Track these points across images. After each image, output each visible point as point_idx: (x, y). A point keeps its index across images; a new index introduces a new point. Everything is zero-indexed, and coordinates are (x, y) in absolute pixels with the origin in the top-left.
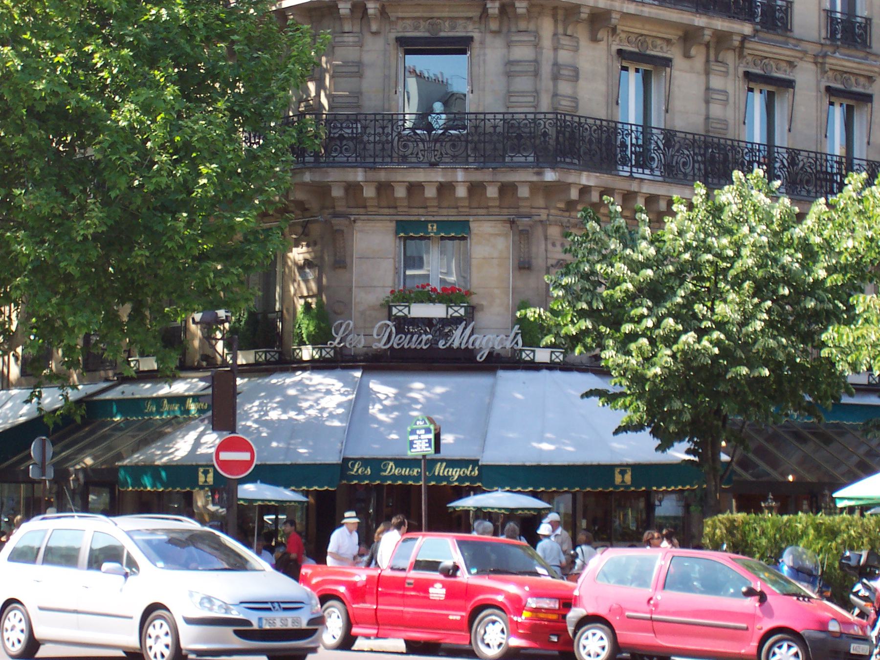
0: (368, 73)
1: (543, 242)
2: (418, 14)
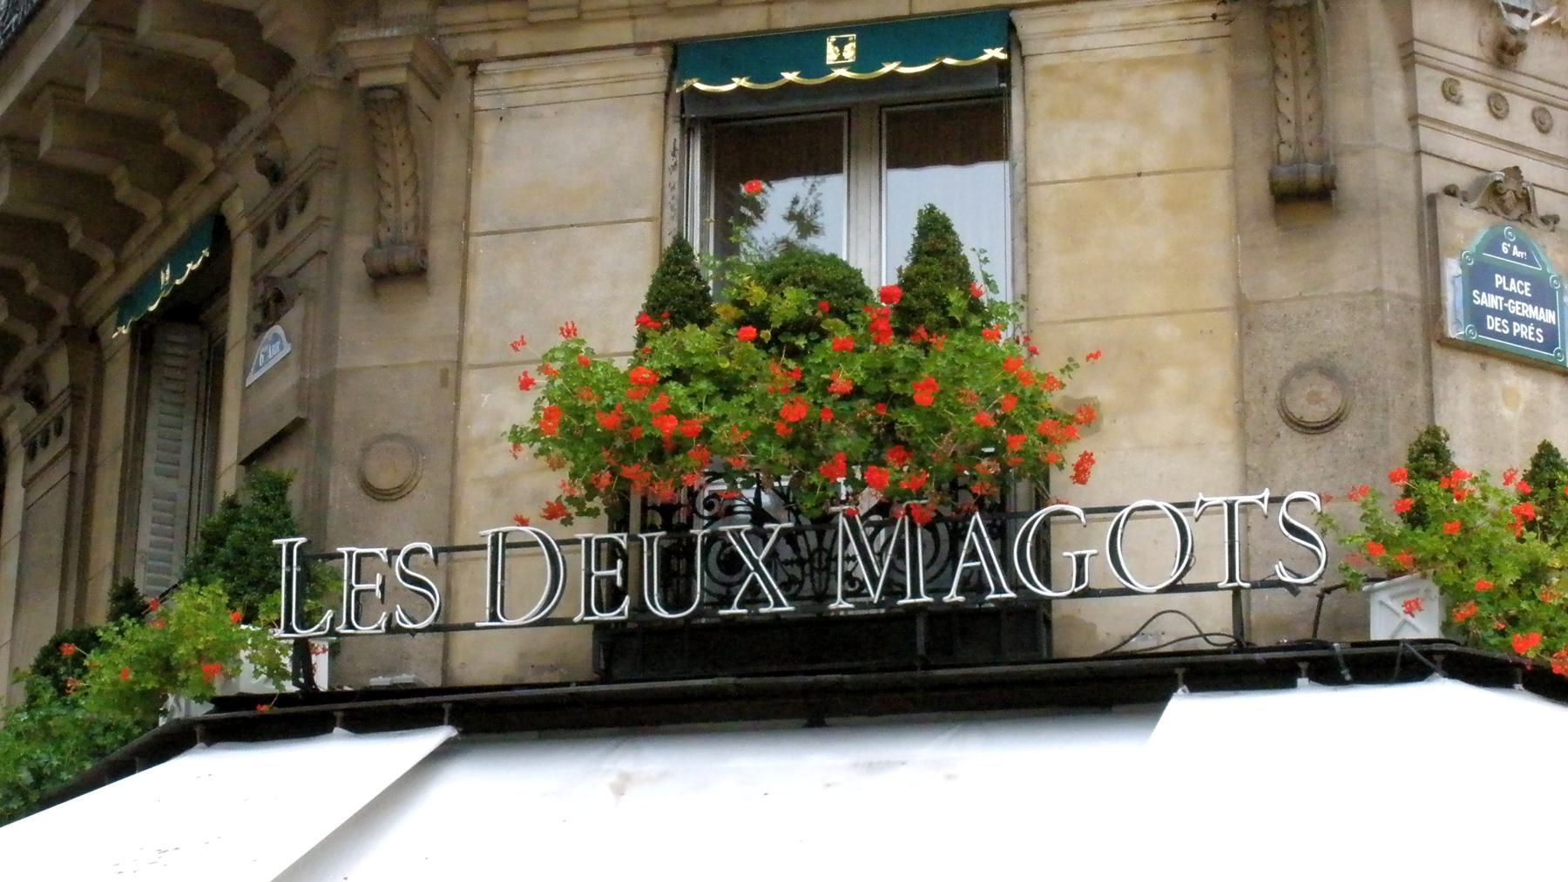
1: (1390, 74)
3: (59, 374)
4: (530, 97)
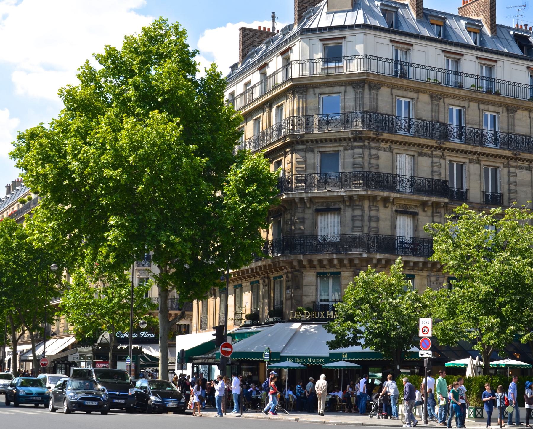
0: (306, 221)
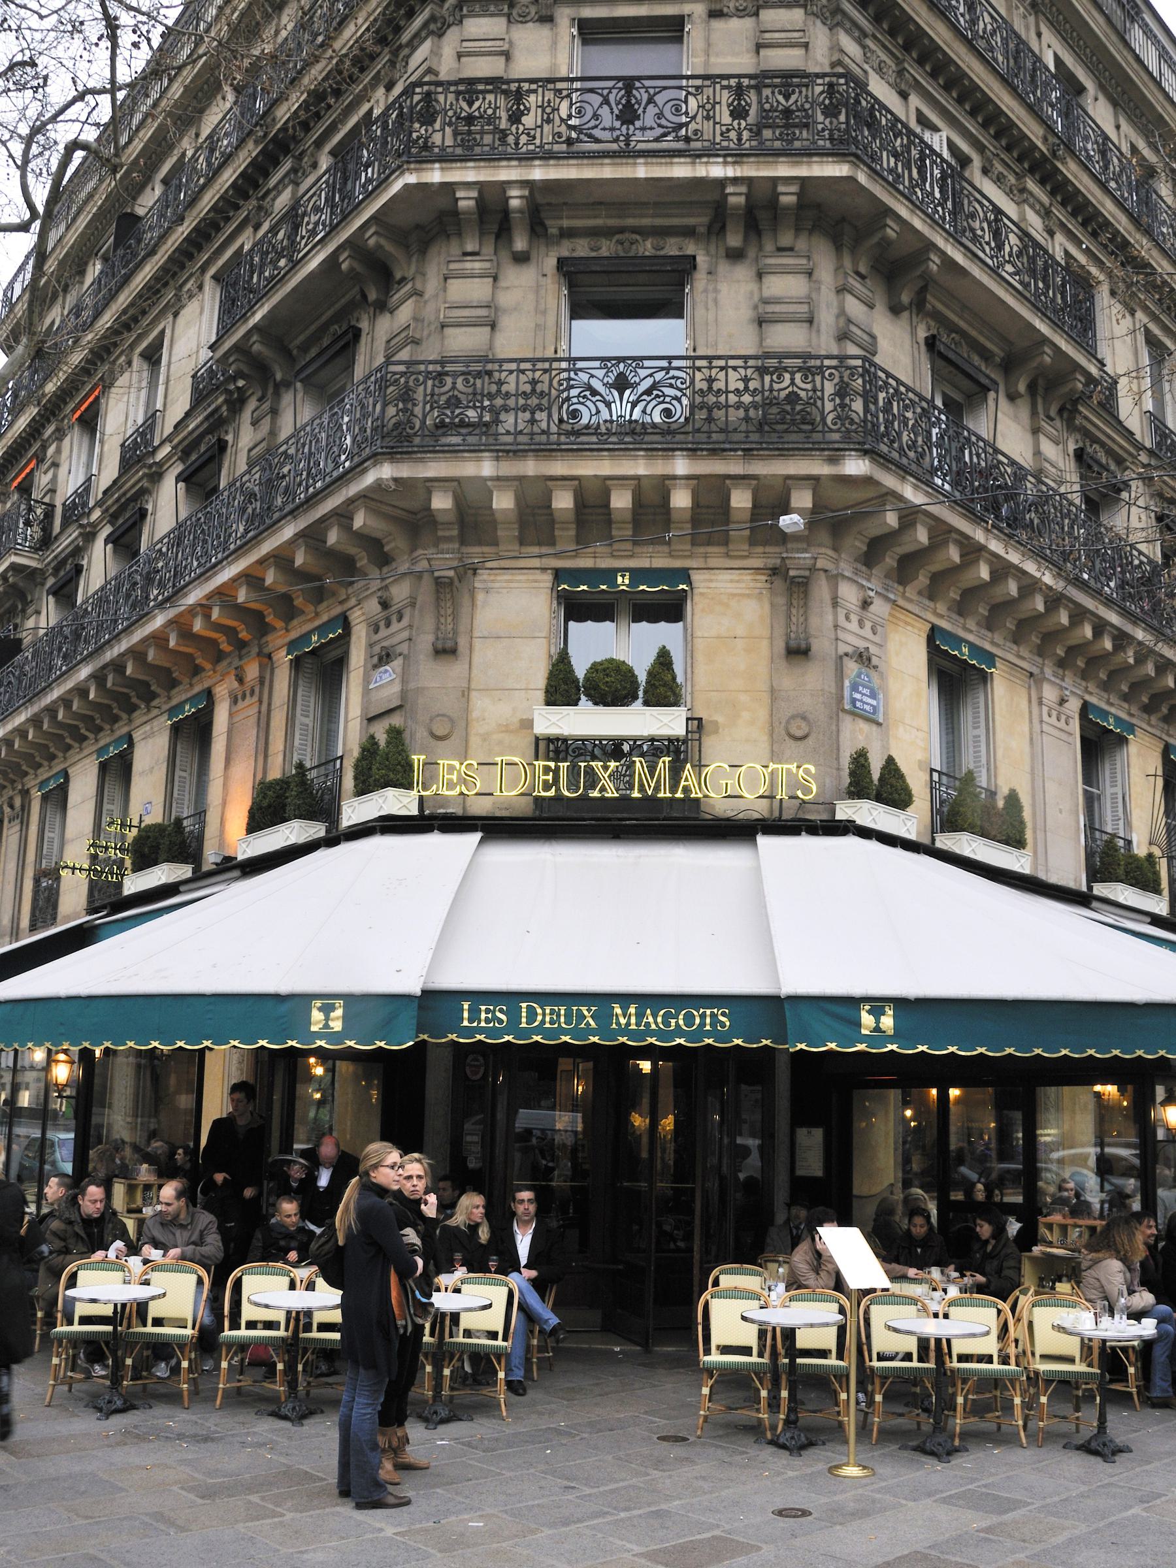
0: (505, 322)
1: (829, 609)
2: (599, 222)
3: (252, 671)
4: (497, 585)
